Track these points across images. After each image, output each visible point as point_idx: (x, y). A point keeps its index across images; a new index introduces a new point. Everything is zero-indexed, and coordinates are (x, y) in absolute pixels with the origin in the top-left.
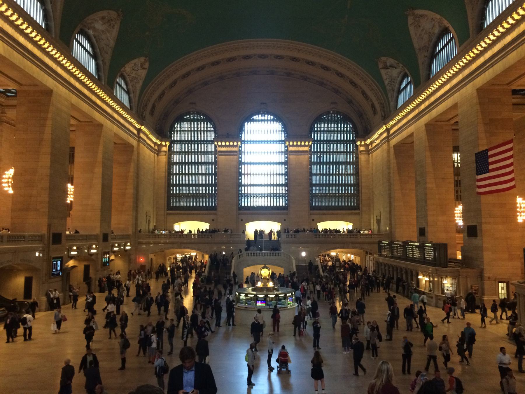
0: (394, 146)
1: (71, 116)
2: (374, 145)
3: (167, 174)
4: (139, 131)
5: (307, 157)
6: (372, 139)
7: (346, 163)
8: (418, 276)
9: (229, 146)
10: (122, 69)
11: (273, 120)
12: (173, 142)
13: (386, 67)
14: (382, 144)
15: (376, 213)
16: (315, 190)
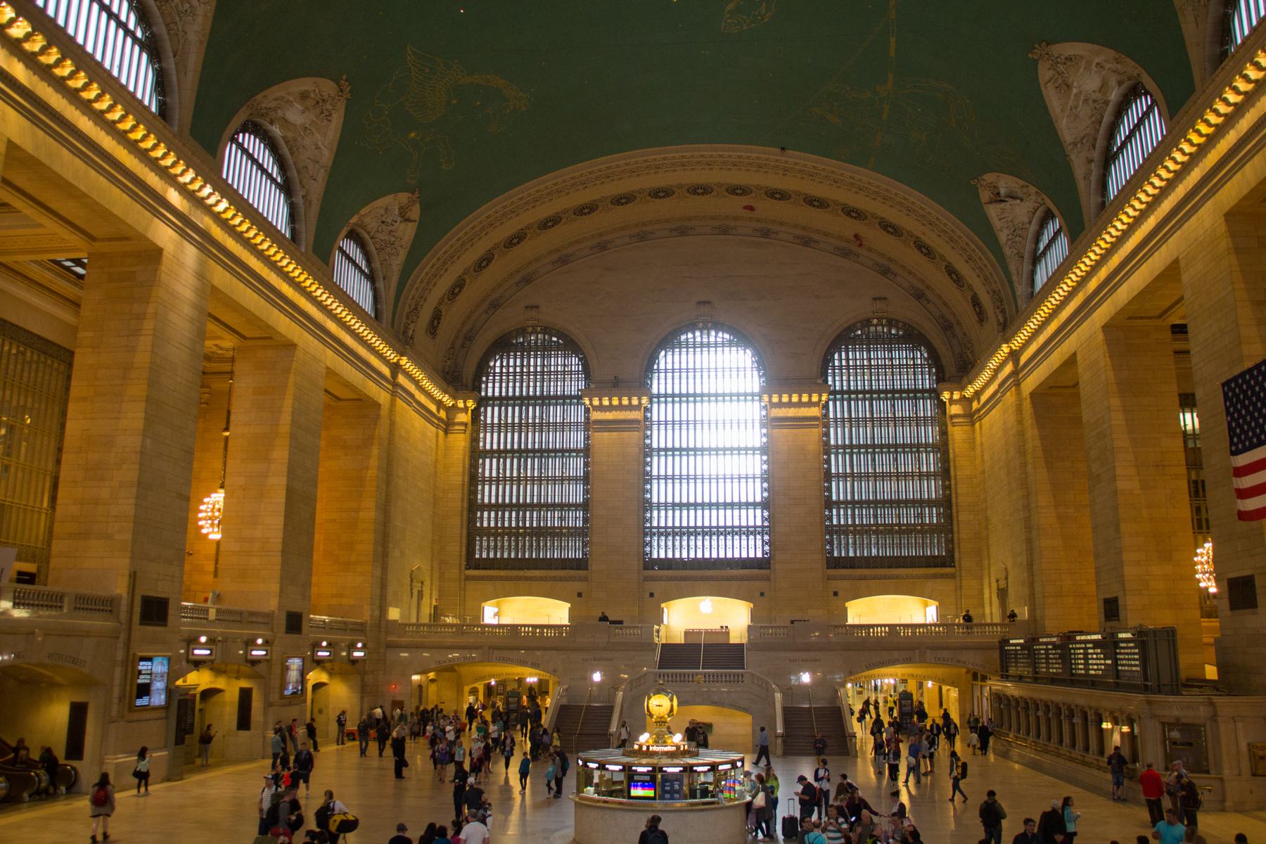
0: (1032, 395)
1: (210, 315)
2: (984, 398)
3: (467, 479)
4: (396, 368)
5: (815, 433)
6: (978, 384)
7: (916, 448)
8: (1101, 723)
9: (621, 407)
10: (354, 220)
11: (731, 344)
12: (483, 402)
13: (998, 199)
14: (1004, 394)
15: (995, 571)
16: (838, 517)
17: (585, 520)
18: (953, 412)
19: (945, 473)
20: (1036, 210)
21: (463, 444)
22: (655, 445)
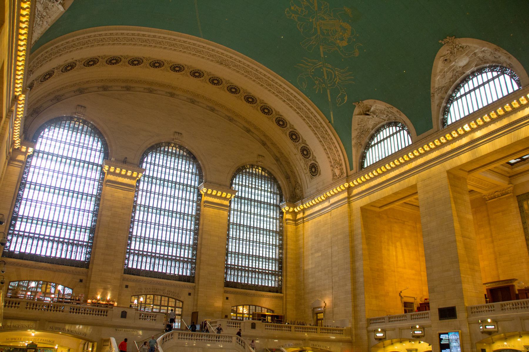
2: (308, 213)
9: (125, 176)
13: (366, 113)
16: (231, 261)
20: (379, 123)
21: (18, 174)
22: (139, 202)
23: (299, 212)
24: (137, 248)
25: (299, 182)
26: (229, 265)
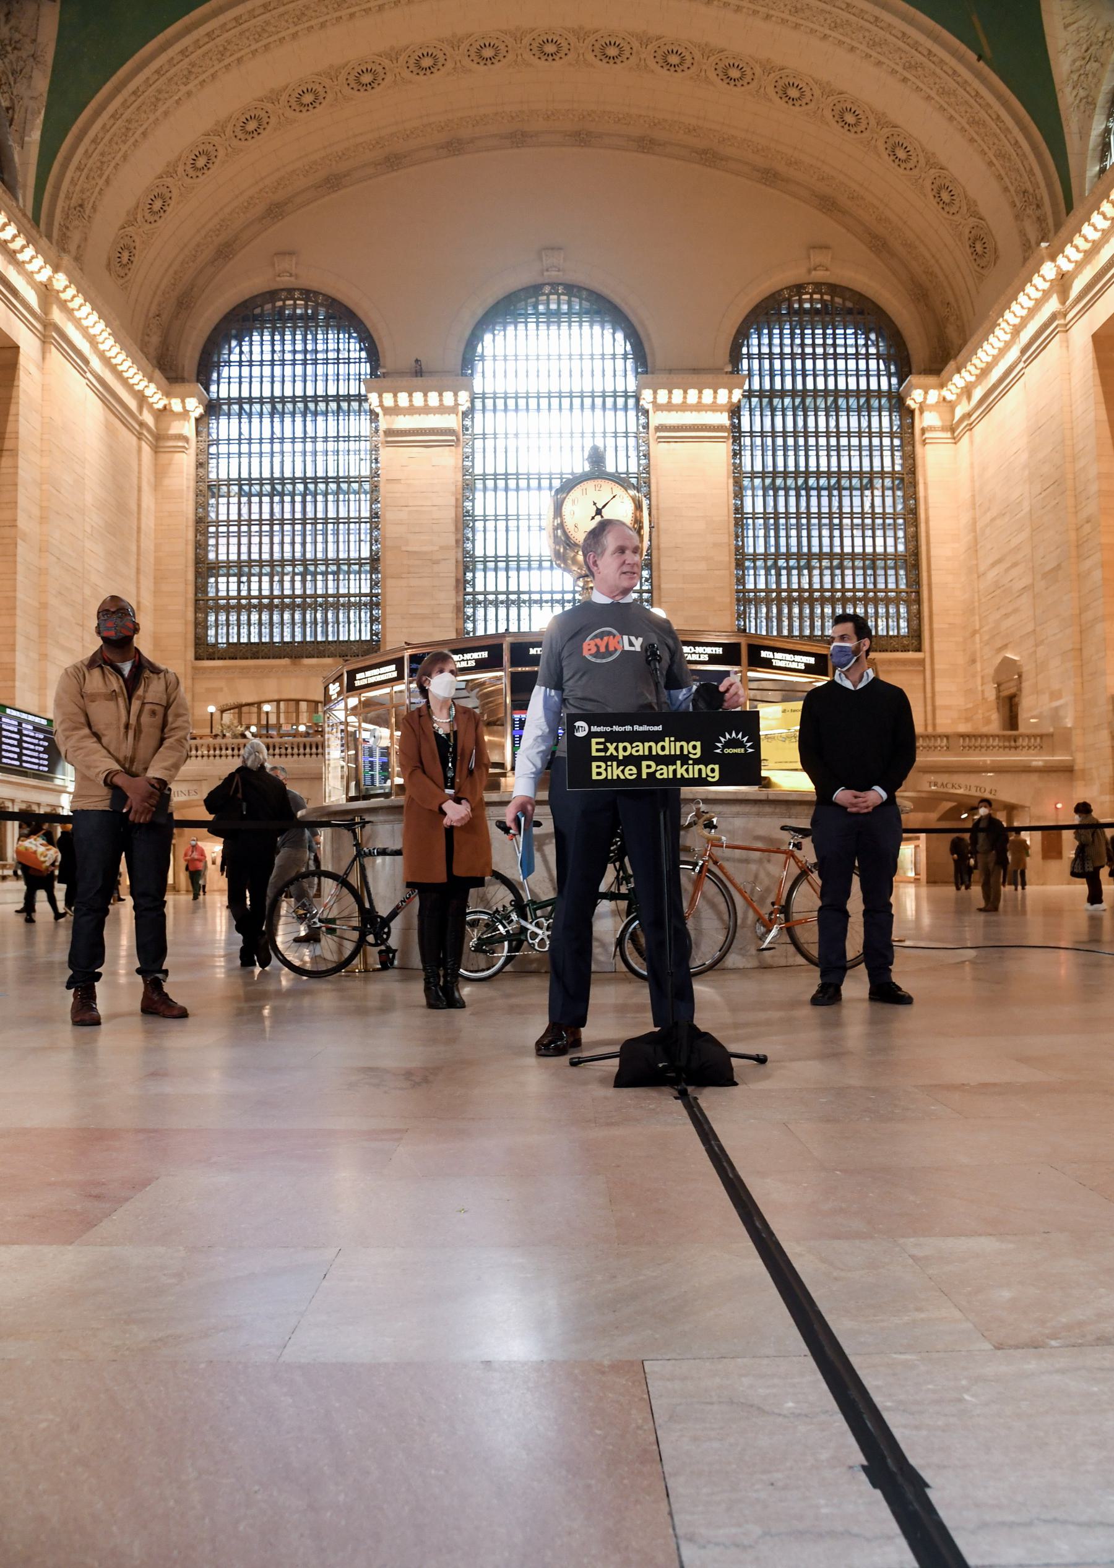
4: (46, 292)
5: (721, 451)
7: (868, 480)
9: (426, 410)
12: (213, 408)
14: (1029, 362)
16: (757, 580)
17: (374, 584)
18: (925, 424)
19: (912, 516)
22: (478, 470)
23: (959, 396)
24: (491, 588)
25: (952, 300)
26: (750, 591)
